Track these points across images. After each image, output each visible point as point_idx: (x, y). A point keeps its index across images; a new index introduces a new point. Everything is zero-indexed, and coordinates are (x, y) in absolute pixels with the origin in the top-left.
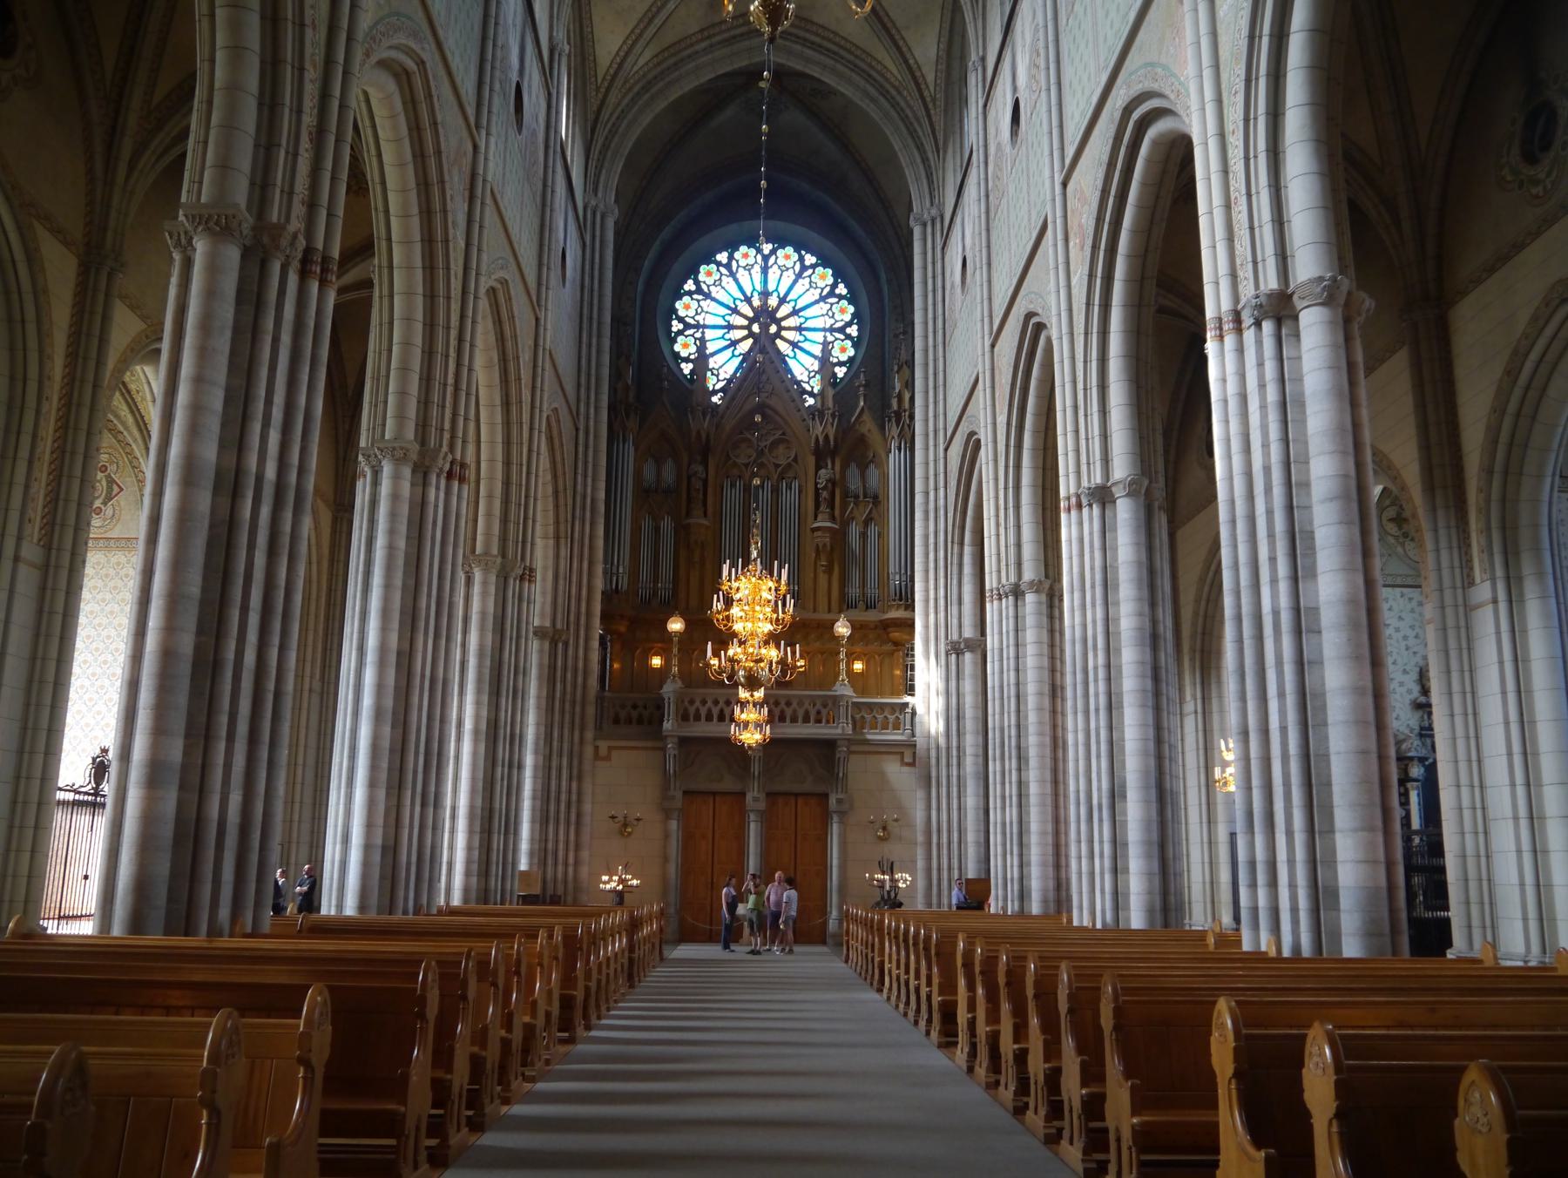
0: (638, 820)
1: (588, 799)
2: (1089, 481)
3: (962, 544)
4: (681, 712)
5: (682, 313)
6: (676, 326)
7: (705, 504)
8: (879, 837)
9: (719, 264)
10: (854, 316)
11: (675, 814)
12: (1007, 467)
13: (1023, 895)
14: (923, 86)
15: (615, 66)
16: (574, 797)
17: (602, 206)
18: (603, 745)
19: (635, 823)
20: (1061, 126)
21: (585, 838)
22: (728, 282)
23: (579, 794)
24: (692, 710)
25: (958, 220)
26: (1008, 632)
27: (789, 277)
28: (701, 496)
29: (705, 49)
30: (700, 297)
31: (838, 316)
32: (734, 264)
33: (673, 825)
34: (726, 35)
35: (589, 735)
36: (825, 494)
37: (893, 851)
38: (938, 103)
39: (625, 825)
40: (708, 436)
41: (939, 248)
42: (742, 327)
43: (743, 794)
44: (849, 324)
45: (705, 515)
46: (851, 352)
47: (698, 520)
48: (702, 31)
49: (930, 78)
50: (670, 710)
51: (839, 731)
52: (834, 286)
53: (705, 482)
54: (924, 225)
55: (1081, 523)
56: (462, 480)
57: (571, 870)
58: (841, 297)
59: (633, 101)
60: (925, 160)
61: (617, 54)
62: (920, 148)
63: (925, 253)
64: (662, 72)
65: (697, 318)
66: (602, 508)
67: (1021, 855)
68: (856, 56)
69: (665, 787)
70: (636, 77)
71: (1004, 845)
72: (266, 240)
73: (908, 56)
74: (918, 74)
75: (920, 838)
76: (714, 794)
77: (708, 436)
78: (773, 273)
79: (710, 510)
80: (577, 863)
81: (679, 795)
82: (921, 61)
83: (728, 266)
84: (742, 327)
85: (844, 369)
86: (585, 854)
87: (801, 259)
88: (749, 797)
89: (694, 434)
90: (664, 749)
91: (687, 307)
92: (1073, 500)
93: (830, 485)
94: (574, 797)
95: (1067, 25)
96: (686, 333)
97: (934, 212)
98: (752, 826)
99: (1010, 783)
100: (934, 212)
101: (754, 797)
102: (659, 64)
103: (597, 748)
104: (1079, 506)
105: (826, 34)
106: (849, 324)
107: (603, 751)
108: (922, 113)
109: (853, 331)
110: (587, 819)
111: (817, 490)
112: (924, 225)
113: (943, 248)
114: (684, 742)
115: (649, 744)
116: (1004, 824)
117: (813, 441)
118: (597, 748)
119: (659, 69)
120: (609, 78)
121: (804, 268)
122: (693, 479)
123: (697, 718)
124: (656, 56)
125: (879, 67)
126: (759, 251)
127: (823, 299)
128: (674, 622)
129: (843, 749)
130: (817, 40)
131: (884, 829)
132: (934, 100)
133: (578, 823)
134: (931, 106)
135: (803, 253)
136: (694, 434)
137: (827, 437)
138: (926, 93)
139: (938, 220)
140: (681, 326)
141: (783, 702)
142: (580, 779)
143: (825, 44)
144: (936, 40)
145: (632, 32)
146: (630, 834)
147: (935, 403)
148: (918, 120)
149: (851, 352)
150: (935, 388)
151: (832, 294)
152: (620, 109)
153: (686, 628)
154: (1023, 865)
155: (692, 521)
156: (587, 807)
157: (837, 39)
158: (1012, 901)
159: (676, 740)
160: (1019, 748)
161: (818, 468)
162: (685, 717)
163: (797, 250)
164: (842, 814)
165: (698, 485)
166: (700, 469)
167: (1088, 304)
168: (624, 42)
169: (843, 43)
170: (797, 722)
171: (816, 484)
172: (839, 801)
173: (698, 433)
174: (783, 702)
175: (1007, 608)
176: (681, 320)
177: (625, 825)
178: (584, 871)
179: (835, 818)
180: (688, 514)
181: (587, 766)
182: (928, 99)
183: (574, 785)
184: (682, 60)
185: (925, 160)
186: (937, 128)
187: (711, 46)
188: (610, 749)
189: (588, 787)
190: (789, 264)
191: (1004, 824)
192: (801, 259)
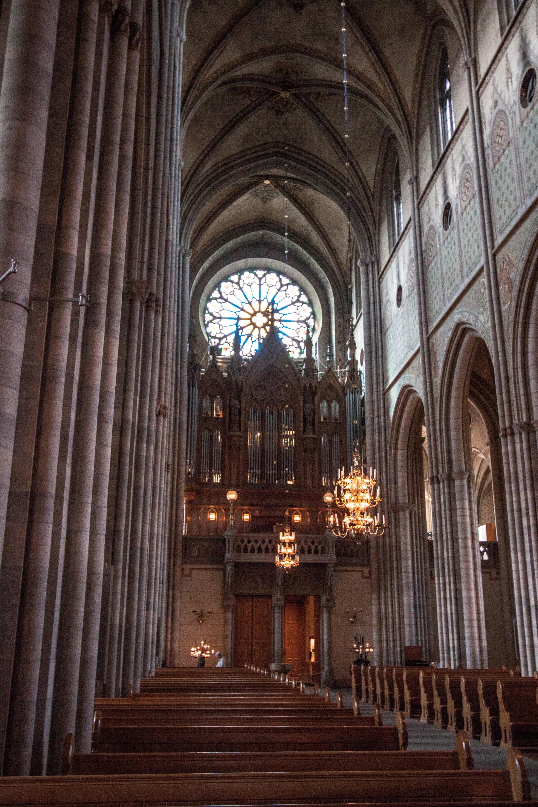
0: (210, 613)
1: (178, 600)
2: (519, 420)
3: (396, 448)
4: (236, 547)
7: (240, 424)
8: (351, 622)
9: (232, 282)
11: (230, 610)
12: (441, 407)
13: (461, 657)
14: (367, 188)
15: (192, 171)
16: (171, 600)
17: (183, 250)
18: (187, 568)
19: (208, 614)
20: (490, 222)
21: (177, 625)
23: (173, 597)
24: (242, 546)
25: (393, 264)
26: (445, 502)
28: (237, 418)
29: (241, 163)
30: (222, 301)
32: (241, 282)
33: (230, 615)
34: (253, 156)
35: (179, 561)
36: (310, 418)
37: (359, 630)
38: (375, 198)
39: (201, 616)
40: (242, 383)
41: (377, 279)
43: (270, 596)
45: (240, 430)
47: (235, 433)
48: (240, 152)
49: (371, 184)
50: (230, 546)
51: (329, 558)
52: (299, 296)
53: (240, 410)
54: (367, 266)
55: (514, 444)
56: (165, 416)
57: (169, 644)
59: (201, 191)
60: (367, 229)
61: (194, 164)
62: (365, 224)
63: (367, 281)
64: (217, 175)
65: (220, 313)
66: (185, 426)
67: (458, 633)
68: (328, 170)
69: (224, 594)
70: (203, 177)
71: (447, 626)
72: (134, 289)
73: (359, 171)
74: (364, 181)
75: (375, 622)
76: (252, 596)
77: (242, 383)
78: (264, 288)
79: (242, 428)
80: (172, 639)
81: (233, 598)
82: (366, 174)
83: (238, 283)
86: (177, 634)
87: (280, 280)
88: (274, 598)
89: (234, 383)
90: (224, 570)
92: (508, 431)
93: (312, 413)
94: (171, 600)
95: (494, 167)
96: (214, 321)
97: (373, 258)
98: (276, 615)
99: (450, 590)
100: (373, 258)
101: (277, 597)
102: (215, 170)
103: (183, 569)
105: (311, 156)
107: (187, 571)
108: (365, 203)
110: (178, 613)
111: (304, 416)
112: (367, 266)
113: (379, 280)
114: (237, 565)
115: (214, 566)
116: (446, 614)
117: (302, 389)
118: (183, 569)
119: (215, 173)
120: (188, 177)
122: (233, 408)
123: (246, 551)
124: (214, 166)
125: (340, 176)
128: (231, 493)
129: (331, 568)
130: (306, 160)
131: (355, 617)
132: (373, 196)
133: (173, 616)
134: (371, 199)
135: (281, 276)
136: (234, 383)
137: (311, 385)
138: (368, 192)
139: (376, 263)
140: (211, 318)
141: (267, 541)
142: (174, 589)
143: (310, 162)
144: (375, 163)
145: (203, 152)
146: (203, 621)
147: (377, 366)
148: (364, 208)
150: (377, 358)
151: (298, 301)
152: (194, 195)
153: (238, 499)
154: (461, 638)
155: (234, 433)
156: (178, 605)
157: (316, 160)
158: (454, 661)
159: (233, 564)
160: (454, 569)
161: (304, 403)
162: (238, 550)
163: (278, 275)
164: (330, 609)
165: (236, 412)
166: (237, 402)
167: (515, 322)
168: (198, 158)
169: (320, 162)
170: (304, 553)
171: (304, 412)
172: (327, 600)
173: (236, 381)
174: (267, 541)
175: (444, 488)
177: (201, 616)
178: (176, 644)
179: (325, 610)
180: (230, 429)
181: (178, 581)
182: (369, 195)
183: (171, 591)
184: (228, 169)
185: (367, 229)
186: (375, 211)
187: (245, 161)
188: (191, 569)
189: (178, 594)
191: (446, 614)
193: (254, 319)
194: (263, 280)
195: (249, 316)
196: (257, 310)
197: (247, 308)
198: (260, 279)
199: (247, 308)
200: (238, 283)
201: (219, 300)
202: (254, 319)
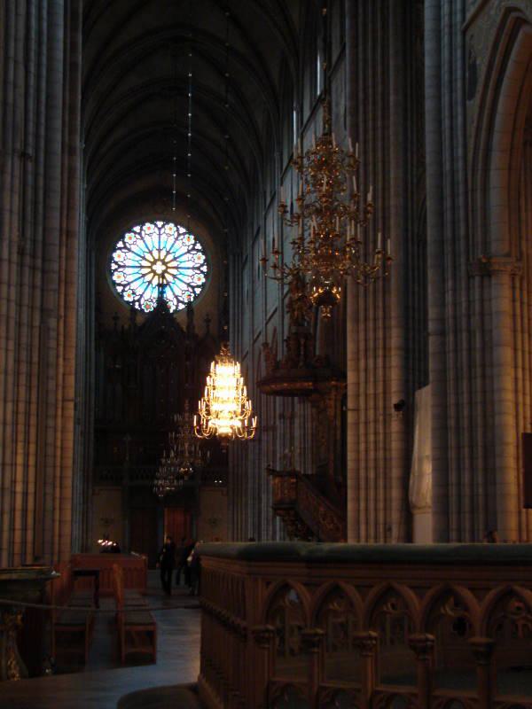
5: (116, 259)
6: (114, 266)
9: (135, 233)
10: (205, 261)
22: (140, 242)
27: (171, 240)
31: (196, 261)
42: (149, 273)
44: (202, 265)
46: (203, 280)
58: (198, 251)
84: (149, 273)
85: (200, 289)
87: (178, 230)
91: (119, 256)
104: (267, 431)
106: (202, 265)
109: (204, 269)
112: (234, 256)
121: (179, 235)
126: (156, 226)
127: (189, 252)
140: (116, 267)
149: (203, 280)
151: (193, 249)
163: (176, 226)
176: (116, 263)
190: (172, 233)
192: (178, 230)
193: (154, 267)
194: (162, 231)
195: (149, 265)
196: (157, 258)
197: (148, 256)
198: (160, 229)
199: (148, 256)
200: (140, 234)
201: (123, 250)
202: (154, 267)
